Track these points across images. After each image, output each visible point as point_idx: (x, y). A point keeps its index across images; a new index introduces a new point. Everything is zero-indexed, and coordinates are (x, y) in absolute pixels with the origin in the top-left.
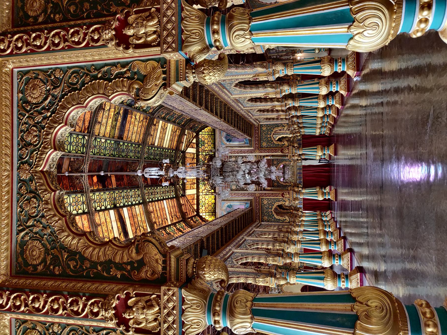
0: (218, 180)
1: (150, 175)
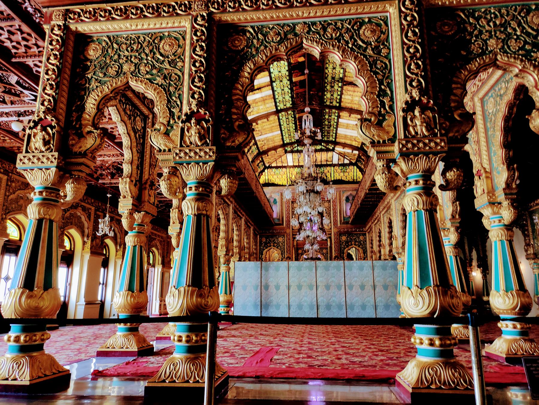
0: (302, 188)
1: (305, 120)
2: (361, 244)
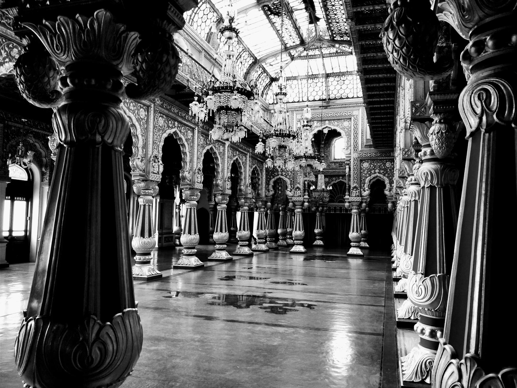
2: (387, 172)
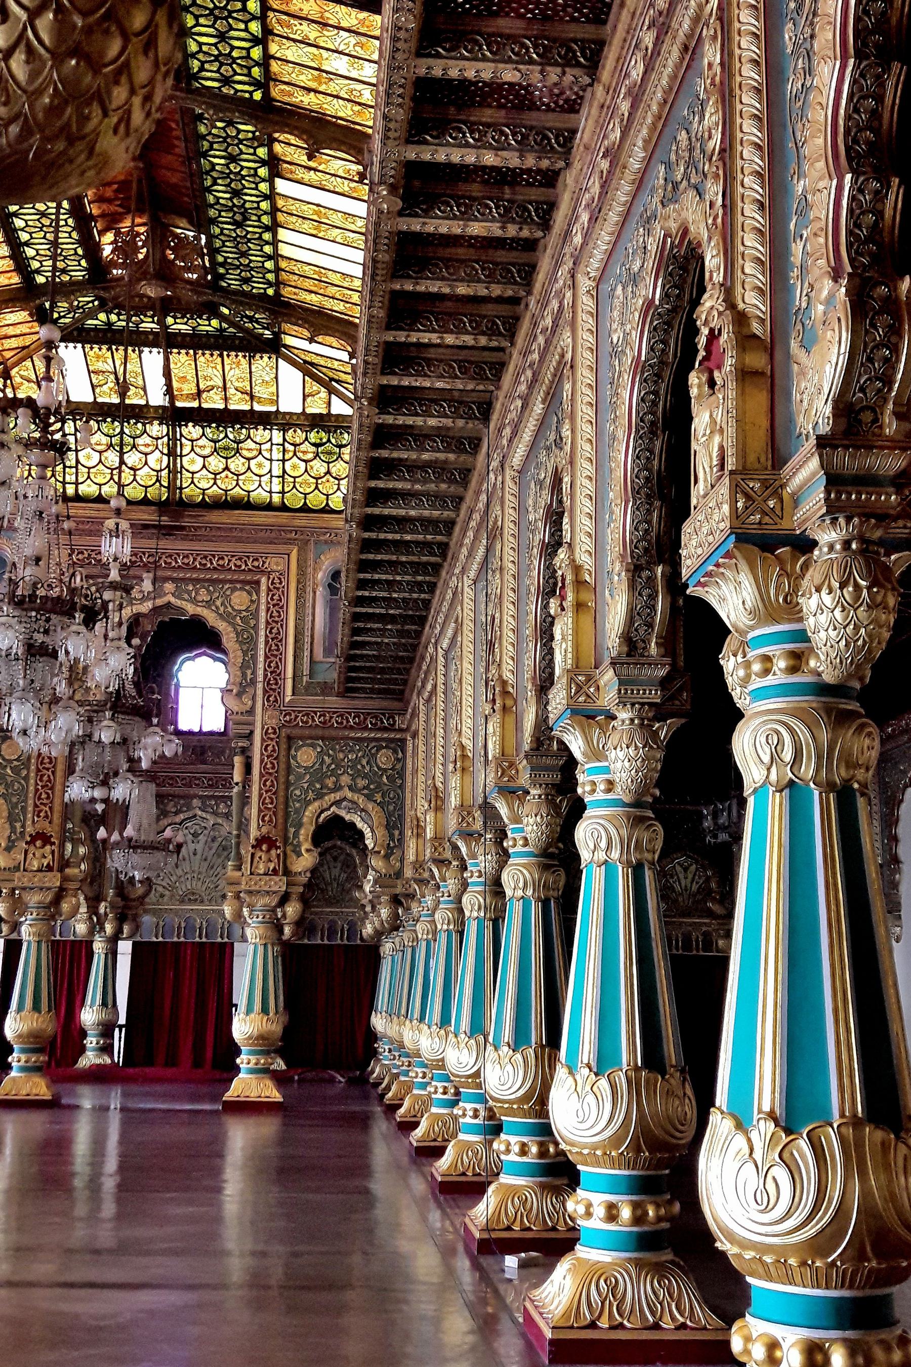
2: (379, 785)
